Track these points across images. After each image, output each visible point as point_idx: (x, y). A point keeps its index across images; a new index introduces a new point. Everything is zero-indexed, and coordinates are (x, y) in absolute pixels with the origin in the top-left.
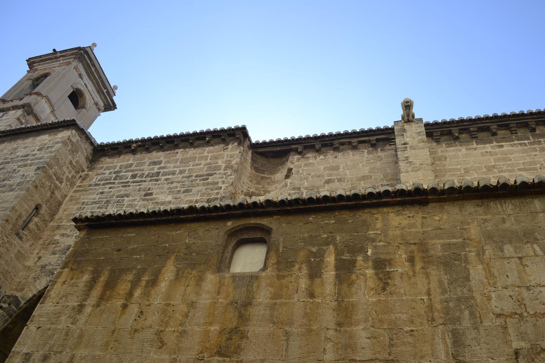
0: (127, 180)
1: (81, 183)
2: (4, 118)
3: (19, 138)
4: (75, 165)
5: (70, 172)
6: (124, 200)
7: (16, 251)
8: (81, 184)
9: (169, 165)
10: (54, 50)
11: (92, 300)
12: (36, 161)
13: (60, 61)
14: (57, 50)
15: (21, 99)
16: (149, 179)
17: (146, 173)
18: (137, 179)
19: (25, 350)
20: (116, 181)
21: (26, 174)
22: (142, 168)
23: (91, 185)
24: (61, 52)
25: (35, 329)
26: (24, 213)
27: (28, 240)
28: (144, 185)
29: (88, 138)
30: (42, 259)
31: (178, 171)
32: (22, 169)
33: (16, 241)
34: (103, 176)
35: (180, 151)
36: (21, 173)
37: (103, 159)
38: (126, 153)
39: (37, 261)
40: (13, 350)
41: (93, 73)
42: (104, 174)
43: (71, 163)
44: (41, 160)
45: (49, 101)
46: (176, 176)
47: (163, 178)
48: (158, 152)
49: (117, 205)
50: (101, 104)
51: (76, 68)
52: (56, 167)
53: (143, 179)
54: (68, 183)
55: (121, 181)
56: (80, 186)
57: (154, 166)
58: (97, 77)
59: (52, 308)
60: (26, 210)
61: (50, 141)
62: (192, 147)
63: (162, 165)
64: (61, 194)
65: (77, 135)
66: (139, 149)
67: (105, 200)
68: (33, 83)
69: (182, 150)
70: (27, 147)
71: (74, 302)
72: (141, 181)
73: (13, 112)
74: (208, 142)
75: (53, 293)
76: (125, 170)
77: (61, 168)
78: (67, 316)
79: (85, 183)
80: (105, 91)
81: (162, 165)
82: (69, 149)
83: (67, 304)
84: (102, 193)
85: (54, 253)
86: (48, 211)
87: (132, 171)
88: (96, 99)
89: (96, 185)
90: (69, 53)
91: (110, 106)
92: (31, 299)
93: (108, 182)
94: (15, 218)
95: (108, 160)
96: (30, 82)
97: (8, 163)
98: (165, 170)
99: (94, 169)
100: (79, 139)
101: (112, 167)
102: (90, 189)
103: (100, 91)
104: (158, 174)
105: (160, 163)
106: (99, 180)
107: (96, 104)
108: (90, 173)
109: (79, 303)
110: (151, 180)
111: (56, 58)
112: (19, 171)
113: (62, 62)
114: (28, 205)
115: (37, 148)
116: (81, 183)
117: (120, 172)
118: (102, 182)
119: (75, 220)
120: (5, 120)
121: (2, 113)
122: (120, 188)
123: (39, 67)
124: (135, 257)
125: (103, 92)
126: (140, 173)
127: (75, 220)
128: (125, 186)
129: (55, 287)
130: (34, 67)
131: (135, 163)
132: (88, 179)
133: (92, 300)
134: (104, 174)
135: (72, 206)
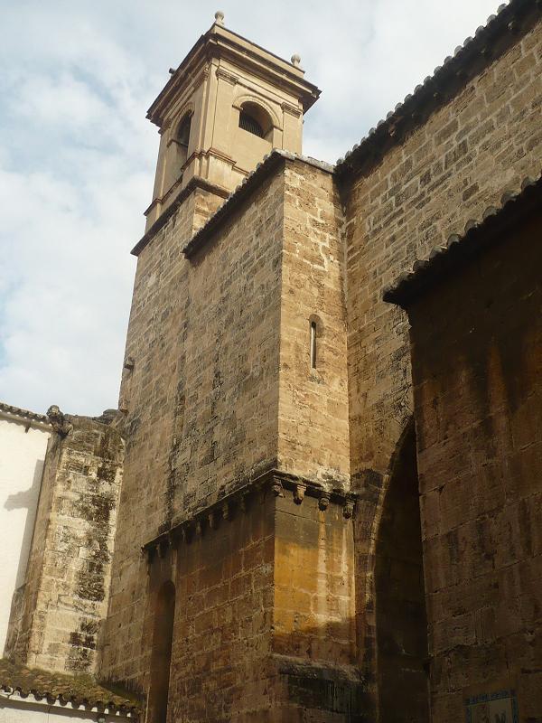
0: (419, 193)
1: (349, 244)
2: (178, 223)
3: (219, 239)
4: (324, 222)
5: (323, 239)
6: (435, 227)
7: (326, 404)
8: (351, 247)
9: (473, 119)
10: (171, 71)
11: (498, 408)
12: (266, 254)
13: (190, 80)
15: (180, 181)
16: (454, 166)
17: (442, 158)
18: (434, 179)
19: (442, 531)
20: (403, 206)
22: (429, 155)
23: (367, 239)
25: (437, 493)
26: (300, 341)
27: (332, 378)
28: (452, 182)
29: (314, 167)
30: (369, 395)
31: (495, 120)
32: (254, 279)
33: (316, 389)
34: (377, 210)
35: (474, 82)
36: (256, 286)
37: (357, 185)
39: (365, 401)
40: (424, 538)
42: (376, 207)
43: (315, 224)
44: (272, 248)
45: (219, 156)
46: (497, 130)
47: (477, 148)
48: (439, 110)
49: (430, 242)
50: (294, 102)
52: (299, 244)
53: (445, 172)
55: (409, 201)
56: (351, 252)
57: (449, 139)
58: (259, 64)
59: (443, 450)
60: (300, 335)
61: (263, 210)
62: (494, 60)
63: (460, 128)
64: (332, 280)
65: (294, 174)
67: (405, 246)
68: (178, 143)
69: (478, 78)
70: (238, 242)
71: (470, 423)
72: (443, 179)
73: (184, 205)
75: (428, 427)
76: (405, 178)
77: (306, 241)
78: (473, 449)
79: (356, 241)
80: (284, 77)
81: (460, 128)
82: (298, 204)
83: (462, 431)
84: (393, 239)
85: (382, 376)
86: (332, 318)
87: (417, 172)
88: (281, 101)
89: (375, 232)
91: (308, 96)
92: (392, 460)
93: (391, 216)
94: (293, 357)
95: (367, 181)
97: (229, 282)
98: (471, 133)
99: (354, 209)
100: (302, 177)
101: (380, 187)
102: (371, 246)
104: (463, 147)
105: (455, 125)
106: (375, 223)
107: (285, 108)
108: (354, 220)
109: (479, 421)
110: (459, 166)
112: (252, 284)
113: (193, 81)
114: (299, 327)
115: (253, 233)
116: (349, 244)
117: (397, 188)
118: (381, 223)
119: (389, 297)
120: (182, 223)
121: (171, 219)
123: (171, 113)
124: (525, 298)
126: (432, 166)
127: (389, 297)
128: (423, 204)
129: (426, 416)
131: (413, 155)
132: (357, 231)
133: (498, 408)
134: (376, 207)
135: (361, 290)
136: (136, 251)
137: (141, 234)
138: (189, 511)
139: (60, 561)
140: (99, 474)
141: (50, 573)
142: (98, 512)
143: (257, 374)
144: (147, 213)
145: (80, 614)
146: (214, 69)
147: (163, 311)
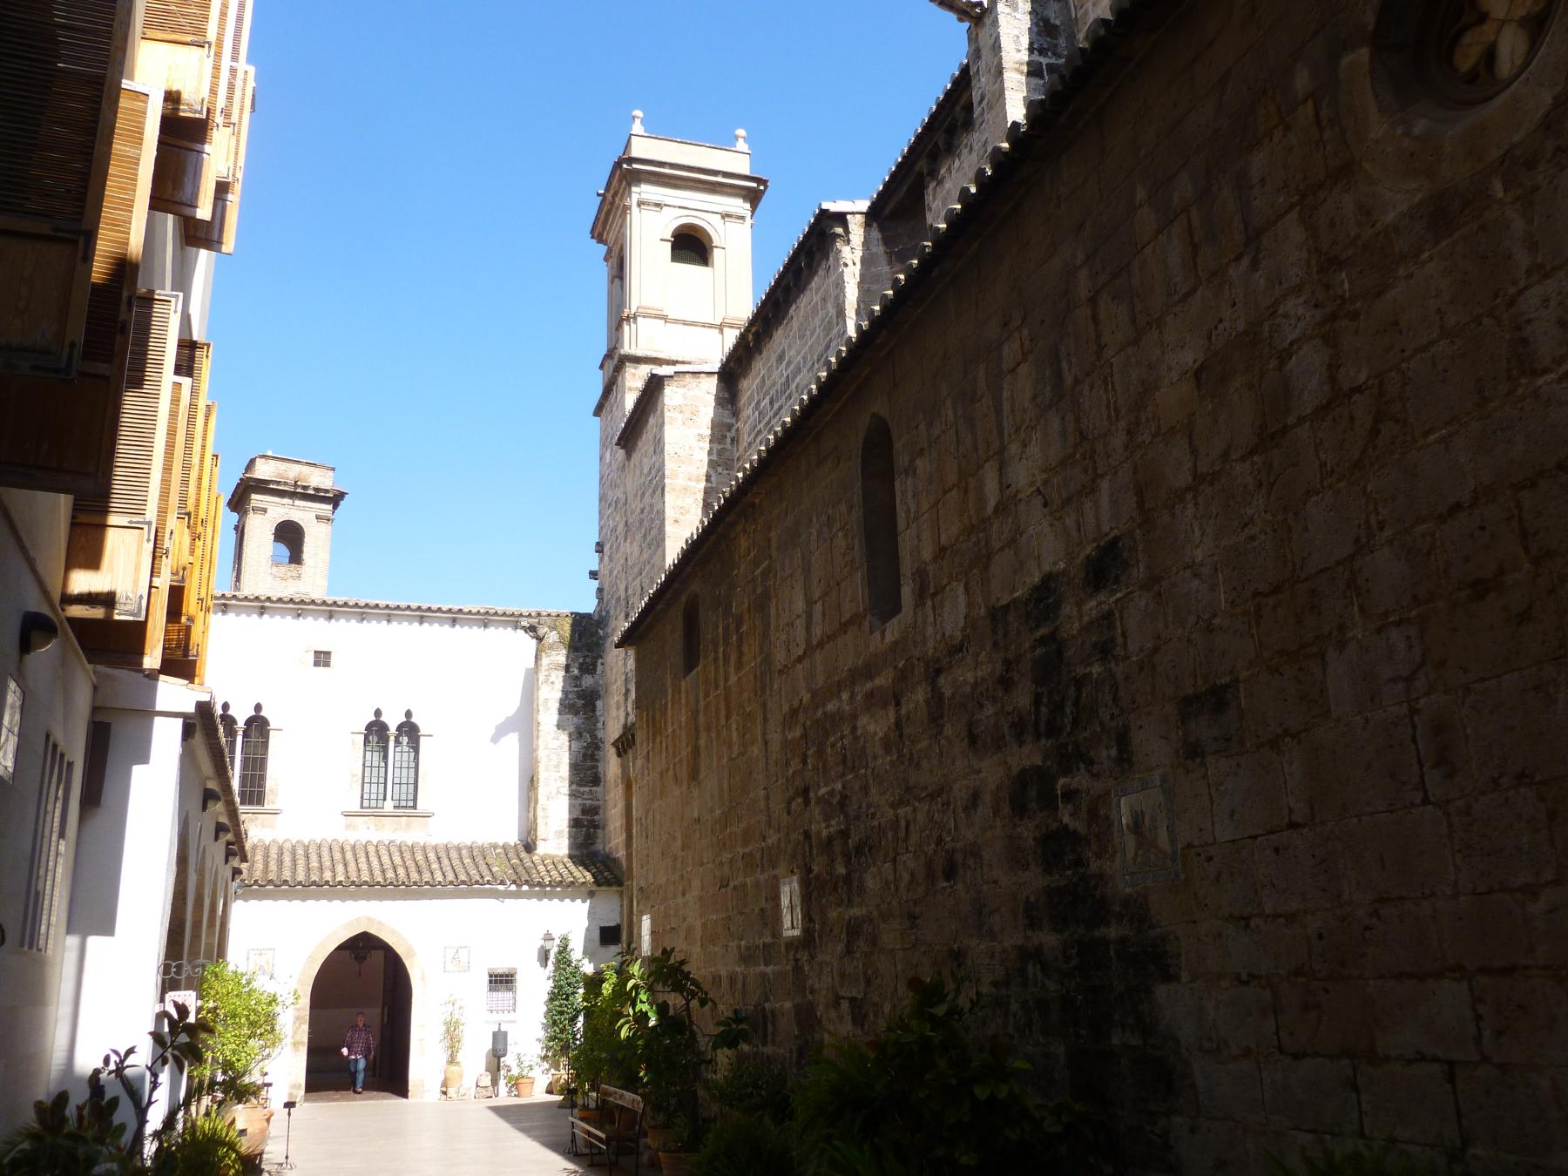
51: (640, 204)
54: (720, 469)
74: (809, 266)
80: (720, 179)
90: (615, 182)
103: (713, 188)
136: (598, 411)
139: (554, 757)
140: (580, 669)
141: (547, 770)
142: (585, 706)
144: (602, 367)
145: (579, 801)
146: (635, 198)
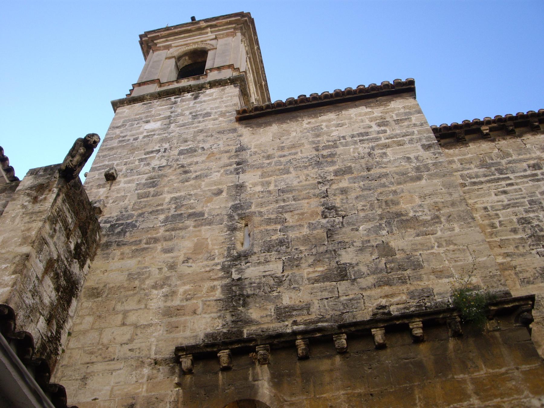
10: (193, 18)
13: (207, 33)
14: (197, 19)
21: (412, 156)
24: (206, 21)
38: (473, 140)
41: (255, 54)
66: (491, 133)
80: (263, 83)
96: (173, 61)
111: (200, 29)
122: (531, 183)
125: (261, 85)
130: (156, 44)
137: (122, 96)
138: (295, 323)
142: (65, 289)
143: (429, 218)
147: (182, 148)
